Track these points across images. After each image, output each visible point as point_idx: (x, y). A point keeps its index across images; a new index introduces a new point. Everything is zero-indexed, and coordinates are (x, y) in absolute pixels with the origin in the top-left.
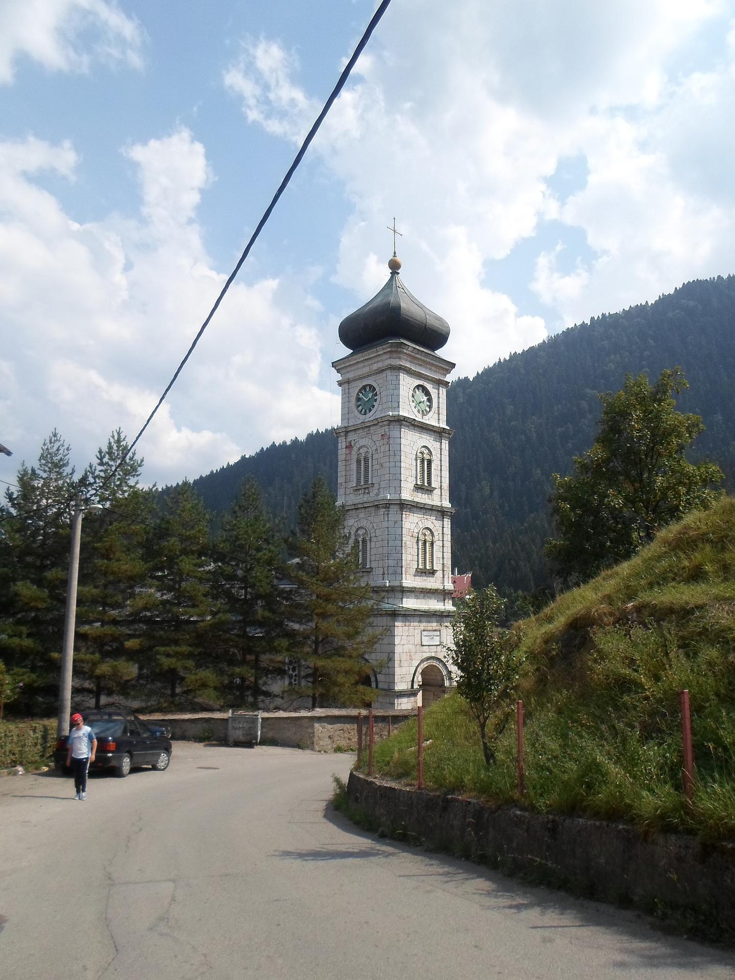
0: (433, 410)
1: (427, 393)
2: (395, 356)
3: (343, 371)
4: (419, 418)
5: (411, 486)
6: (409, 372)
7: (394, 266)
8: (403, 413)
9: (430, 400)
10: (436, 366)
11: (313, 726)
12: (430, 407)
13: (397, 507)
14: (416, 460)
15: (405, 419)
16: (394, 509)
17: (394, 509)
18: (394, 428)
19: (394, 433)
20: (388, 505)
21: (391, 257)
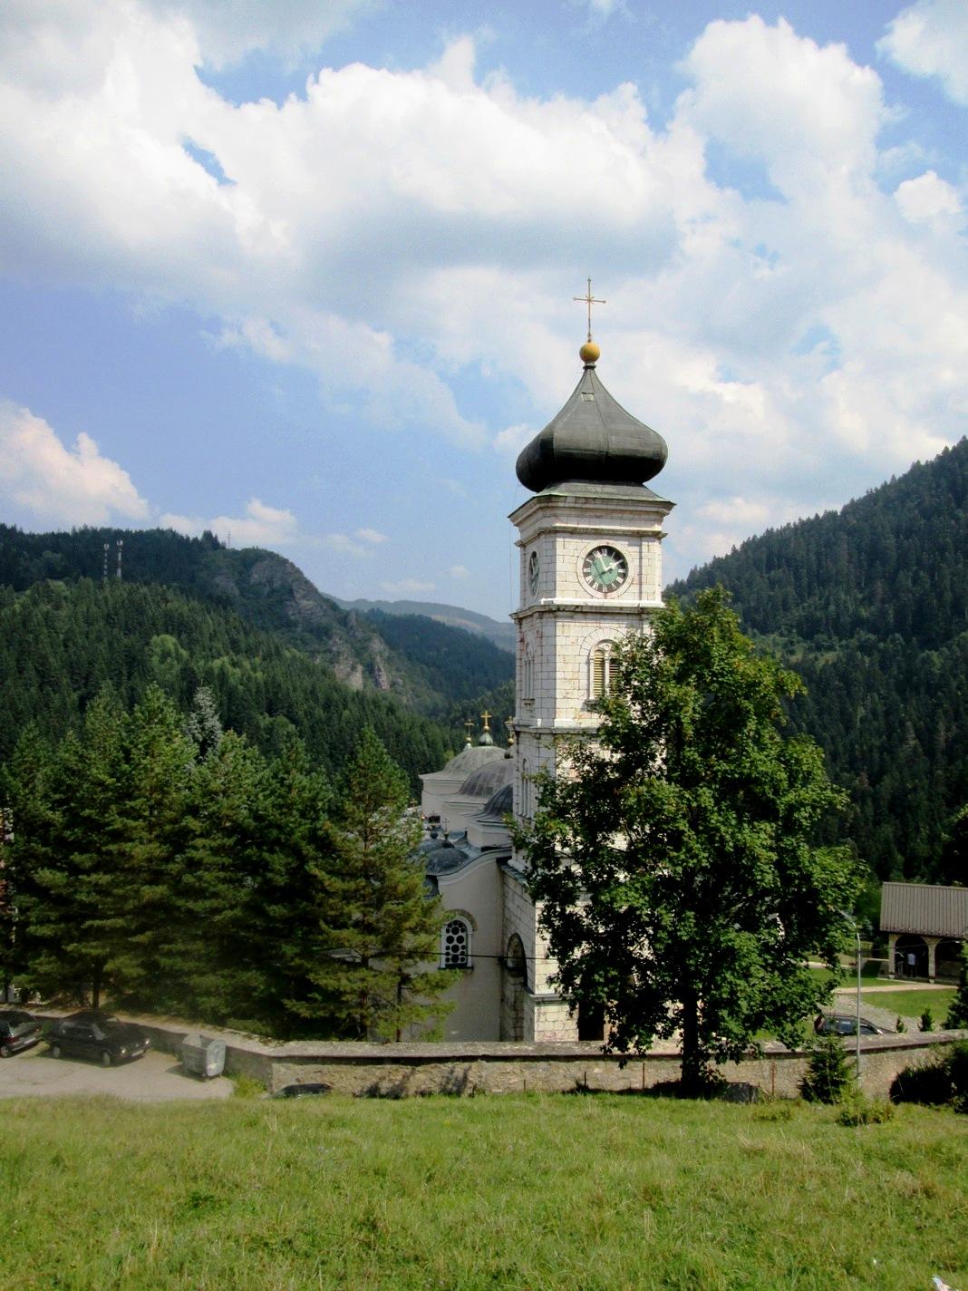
0: (629, 580)
1: (618, 556)
2: (548, 512)
4: (598, 600)
5: (579, 704)
6: (573, 532)
7: (589, 358)
8: (560, 599)
9: (624, 565)
10: (631, 512)
11: (271, 1066)
12: (624, 576)
13: (550, 739)
14: (588, 663)
15: (559, 609)
16: (547, 740)
17: (547, 740)
18: (548, 619)
19: (547, 631)
20: (538, 735)
21: (583, 343)
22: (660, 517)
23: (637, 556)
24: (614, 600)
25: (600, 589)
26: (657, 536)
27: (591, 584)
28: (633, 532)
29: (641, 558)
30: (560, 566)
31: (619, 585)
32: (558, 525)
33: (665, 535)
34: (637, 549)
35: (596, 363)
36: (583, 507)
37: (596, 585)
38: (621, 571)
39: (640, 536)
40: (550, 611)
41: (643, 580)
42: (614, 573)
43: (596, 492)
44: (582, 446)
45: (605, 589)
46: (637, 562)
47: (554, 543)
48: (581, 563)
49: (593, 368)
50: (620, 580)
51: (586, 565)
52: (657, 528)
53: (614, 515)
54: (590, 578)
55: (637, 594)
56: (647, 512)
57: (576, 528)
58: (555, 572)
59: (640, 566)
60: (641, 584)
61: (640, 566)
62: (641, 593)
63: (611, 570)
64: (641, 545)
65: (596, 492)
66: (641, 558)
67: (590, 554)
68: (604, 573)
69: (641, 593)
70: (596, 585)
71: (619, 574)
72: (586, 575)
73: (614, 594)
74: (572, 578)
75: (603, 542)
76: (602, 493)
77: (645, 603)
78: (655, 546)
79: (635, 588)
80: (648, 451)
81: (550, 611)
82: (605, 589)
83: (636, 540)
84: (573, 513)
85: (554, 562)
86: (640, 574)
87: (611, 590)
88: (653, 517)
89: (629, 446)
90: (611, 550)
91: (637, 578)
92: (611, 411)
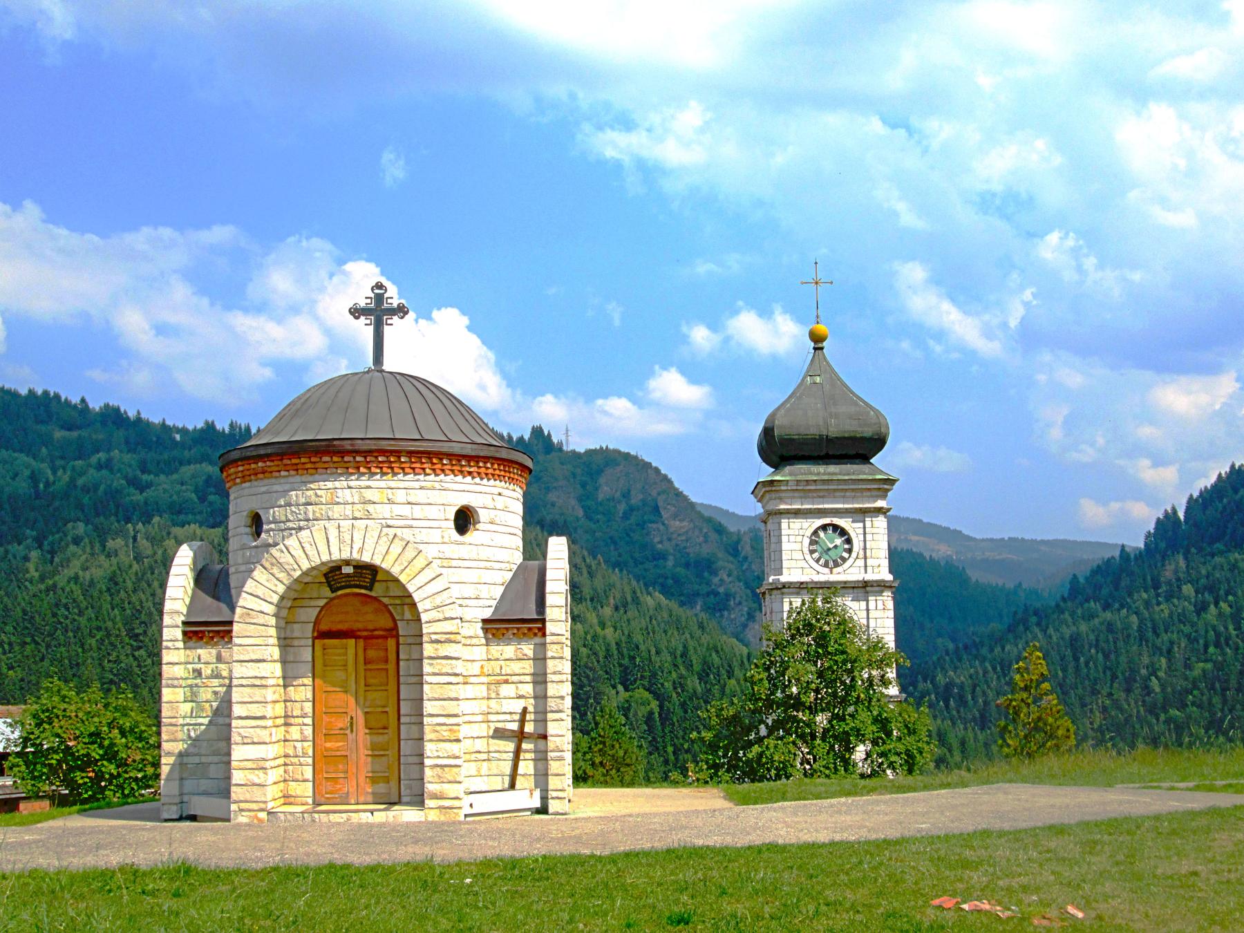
0: (854, 555)
1: (843, 532)
3: (765, 501)
4: (824, 576)
6: (797, 514)
8: (784, 578)
9: (849, 541)
12: (850, 551)
15: (784, 586)
22: (883, 494)
23: (861, 531)
24: (838, 575)
25: (826, 565)
26: (879, 511)
27: (817, 561)
28: (856, 509)
29: (865, 534)
30: (785, 546)
31: (844, 560)
32: (782, 507)
33: (889, 510)
34: (861, 525)
35: (825, 344)
36: (804, 489)
37: (822, 561)
38: (846, 546)
39: (861, 514)
40: (777, 589)
41: (868, 554)
42: (840, 550)
43: (818, 474)
44: (803, 431)
45: (831, 564)
46: (861, 537)
47: (780, 524)
48: (807, 541)
49: (822, 349)
50: (846, 555)
51: (812, 542)
52: (881, 503)
53: (838, 494)
54: (816, 555)
55: (863, 570)
56: (869, 490)
57: (799, 510)
58: (781, 551)
59: (865, 541)
60: (865, 558)
61: (865, 541)
62: (866, 566)
63: (836, 547)
64: (864, 522)
65: (818, 474)
66: (865, 534)
67: (815, 533)
68: (829, 549)
69: (866, 566)
70: (822, 561)
71: (845, 550)
72: (812, 552)
73: (839, 569)
74: (799, 555)
75: (827, 521)
76: (824, 474)
77: (870, 577)
78: (881, 523)
79: (861, 562)
80: (868, 432)
81: (777, 589)
82: (831, 564)
83: (860, 517)
84: (796, 494)
85: (780, 542)
86: (865, 549)
87: (836, 565)
88: (874, 493)
89: (848, 428)
90: (836, 528)
91: (862, 553)
92: (836, 390)
